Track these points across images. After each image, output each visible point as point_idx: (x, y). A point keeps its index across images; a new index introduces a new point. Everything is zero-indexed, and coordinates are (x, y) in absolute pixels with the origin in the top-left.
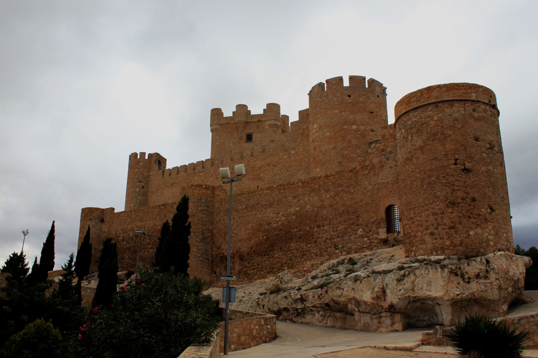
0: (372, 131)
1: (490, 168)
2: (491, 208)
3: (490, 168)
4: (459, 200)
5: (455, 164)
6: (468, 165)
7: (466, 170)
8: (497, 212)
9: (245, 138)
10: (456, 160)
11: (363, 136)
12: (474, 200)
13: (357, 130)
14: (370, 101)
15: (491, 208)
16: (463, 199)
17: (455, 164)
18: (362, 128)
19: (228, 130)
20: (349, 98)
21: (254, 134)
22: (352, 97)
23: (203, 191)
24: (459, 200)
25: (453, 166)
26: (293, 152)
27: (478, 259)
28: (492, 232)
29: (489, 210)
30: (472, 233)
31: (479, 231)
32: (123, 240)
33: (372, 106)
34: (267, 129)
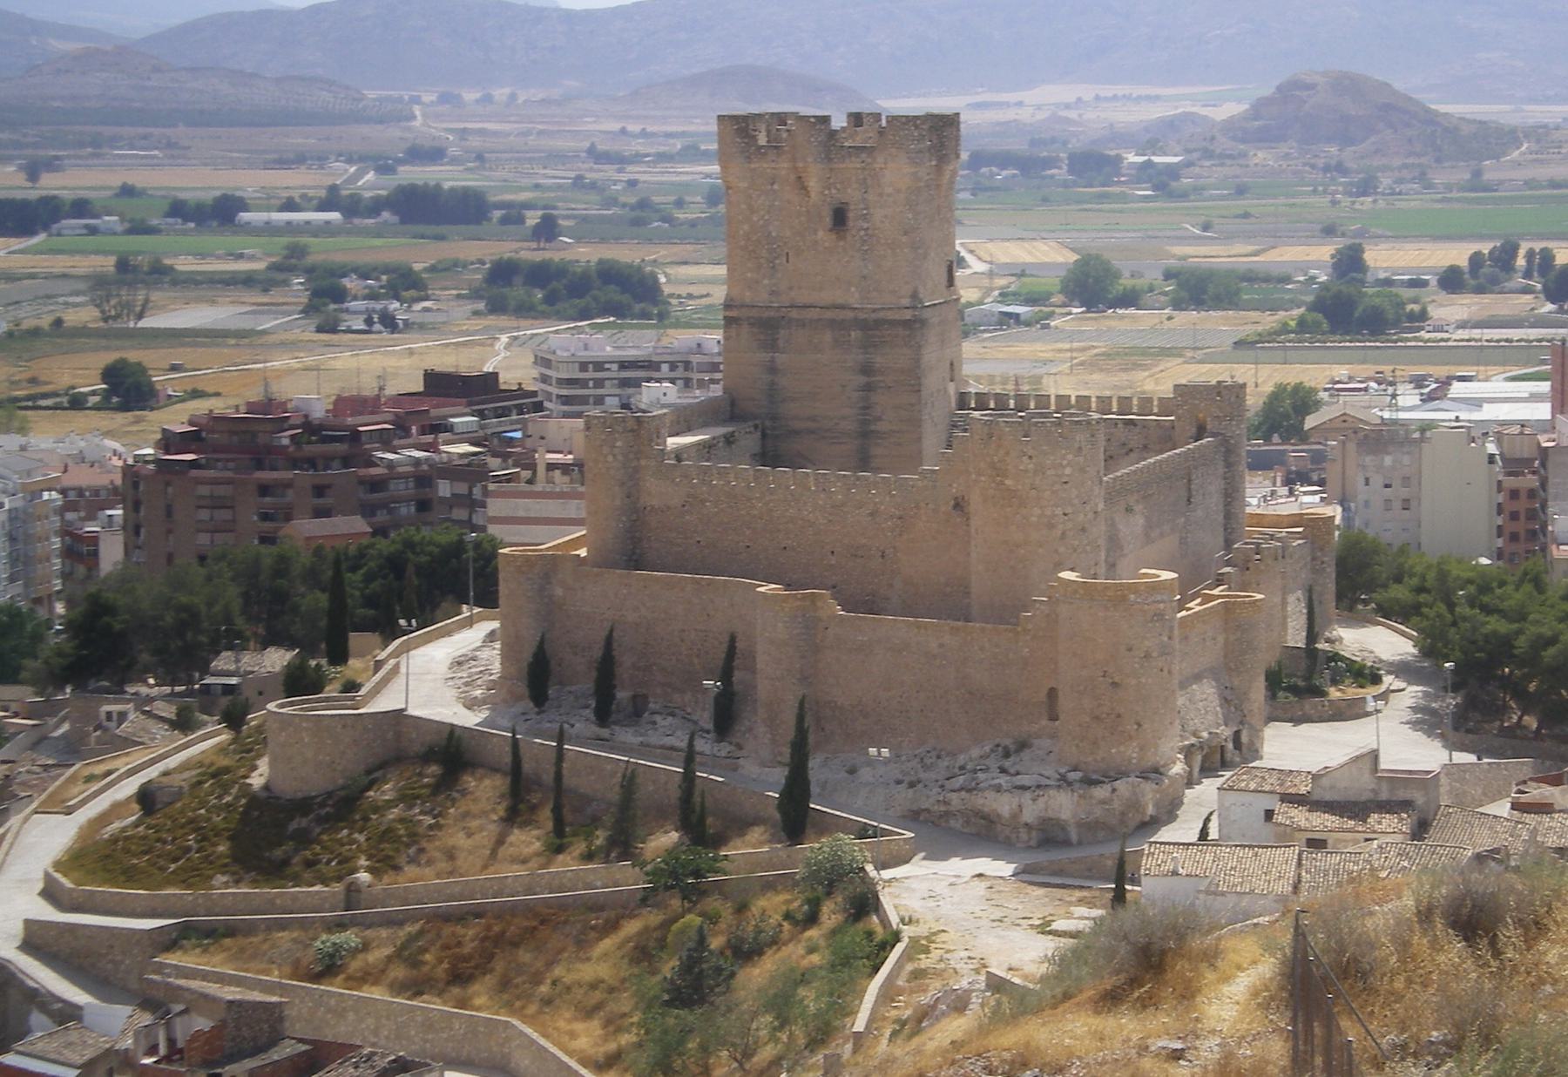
2: (1139, 725)
3: (1143, 680)
4: (1104, 716)
5: (1104, 676)
6: (1116, 680)
7: (1115, 685)
8: (1145, 726)
10: (1105, 672)
12: (1119, 716)
14: (1065, 462)
15: (1139, 725)
16: (1108, 714)
17: (1104, 676)
20: (1029, 461)
22: (1034, 460)
23: (799, 603)
24: (1104, 716)
25: (1101, 679)
27: (1105, 786)
28: (1137, 750)
29: (1136, 727)
31: (1122, 749)
34: (889, 195)
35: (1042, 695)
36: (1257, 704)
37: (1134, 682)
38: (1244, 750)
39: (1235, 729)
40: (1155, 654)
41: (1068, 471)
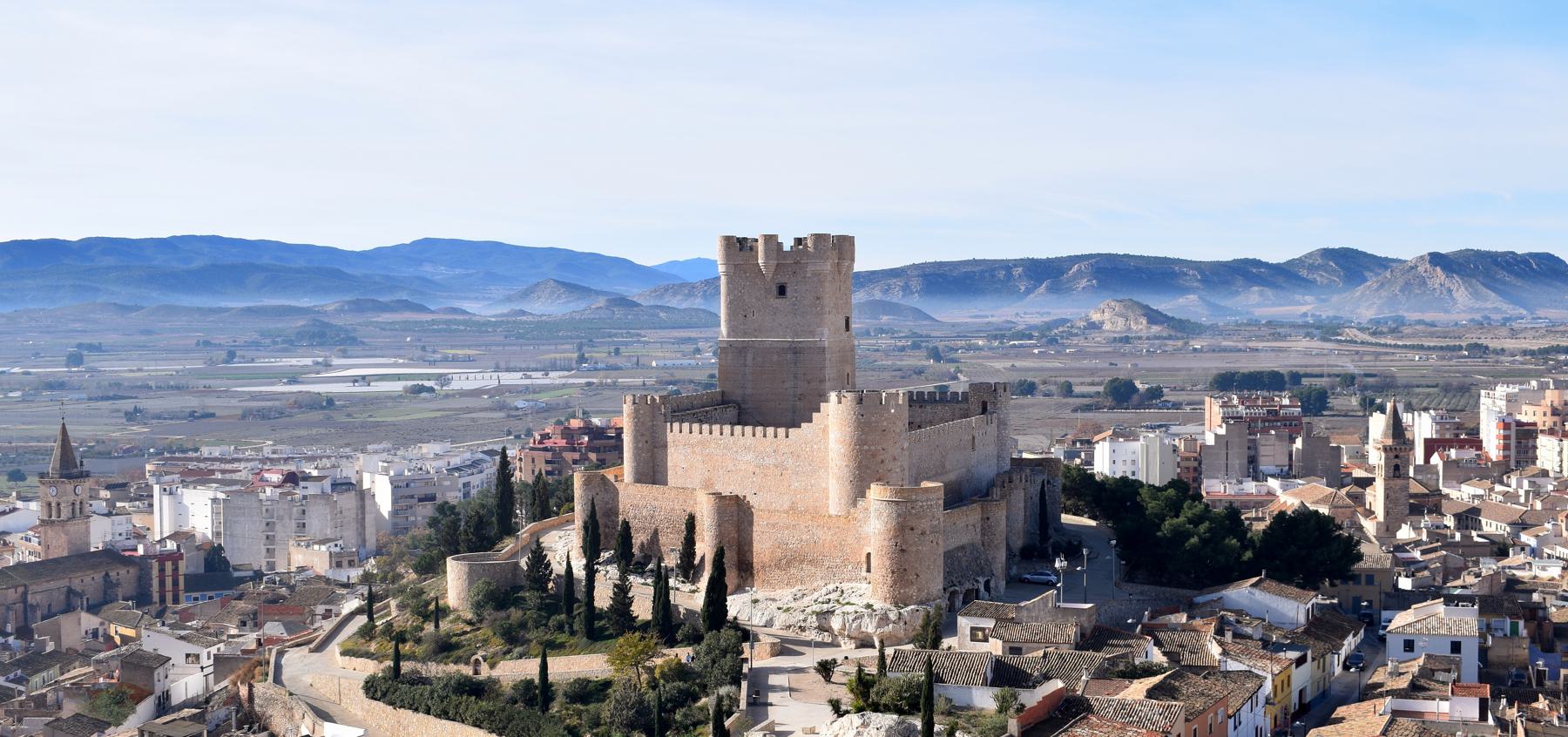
0: (883, 449)
1: (920, 548)
3: (920, 548)
9: (775, 290)
11: (874, 456)
12: (905, 570)
13: (867, 451)
18: (873, 448)
19: (748, 275)
21: (788, 285)
26: (815, 446)
30: (902, 591)
31: (907, 590)
32: (635, 517)
33: (885, 424)
34: (809, 278)
35: (864, 559)
36: (1000, 565)
37: (914, 549)
38: (992, 592)
39: (986, 579)
40: (928, 533)
41: (885, 424)
